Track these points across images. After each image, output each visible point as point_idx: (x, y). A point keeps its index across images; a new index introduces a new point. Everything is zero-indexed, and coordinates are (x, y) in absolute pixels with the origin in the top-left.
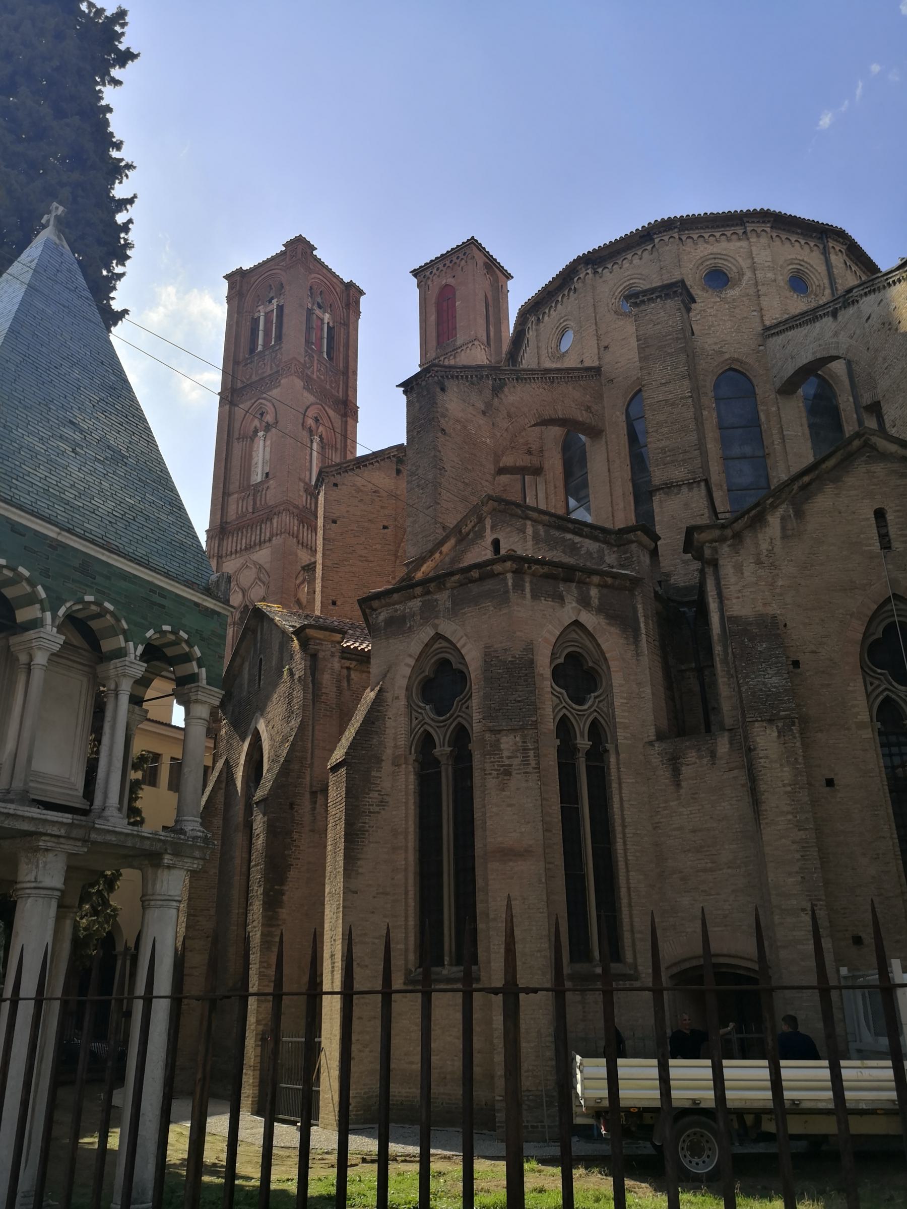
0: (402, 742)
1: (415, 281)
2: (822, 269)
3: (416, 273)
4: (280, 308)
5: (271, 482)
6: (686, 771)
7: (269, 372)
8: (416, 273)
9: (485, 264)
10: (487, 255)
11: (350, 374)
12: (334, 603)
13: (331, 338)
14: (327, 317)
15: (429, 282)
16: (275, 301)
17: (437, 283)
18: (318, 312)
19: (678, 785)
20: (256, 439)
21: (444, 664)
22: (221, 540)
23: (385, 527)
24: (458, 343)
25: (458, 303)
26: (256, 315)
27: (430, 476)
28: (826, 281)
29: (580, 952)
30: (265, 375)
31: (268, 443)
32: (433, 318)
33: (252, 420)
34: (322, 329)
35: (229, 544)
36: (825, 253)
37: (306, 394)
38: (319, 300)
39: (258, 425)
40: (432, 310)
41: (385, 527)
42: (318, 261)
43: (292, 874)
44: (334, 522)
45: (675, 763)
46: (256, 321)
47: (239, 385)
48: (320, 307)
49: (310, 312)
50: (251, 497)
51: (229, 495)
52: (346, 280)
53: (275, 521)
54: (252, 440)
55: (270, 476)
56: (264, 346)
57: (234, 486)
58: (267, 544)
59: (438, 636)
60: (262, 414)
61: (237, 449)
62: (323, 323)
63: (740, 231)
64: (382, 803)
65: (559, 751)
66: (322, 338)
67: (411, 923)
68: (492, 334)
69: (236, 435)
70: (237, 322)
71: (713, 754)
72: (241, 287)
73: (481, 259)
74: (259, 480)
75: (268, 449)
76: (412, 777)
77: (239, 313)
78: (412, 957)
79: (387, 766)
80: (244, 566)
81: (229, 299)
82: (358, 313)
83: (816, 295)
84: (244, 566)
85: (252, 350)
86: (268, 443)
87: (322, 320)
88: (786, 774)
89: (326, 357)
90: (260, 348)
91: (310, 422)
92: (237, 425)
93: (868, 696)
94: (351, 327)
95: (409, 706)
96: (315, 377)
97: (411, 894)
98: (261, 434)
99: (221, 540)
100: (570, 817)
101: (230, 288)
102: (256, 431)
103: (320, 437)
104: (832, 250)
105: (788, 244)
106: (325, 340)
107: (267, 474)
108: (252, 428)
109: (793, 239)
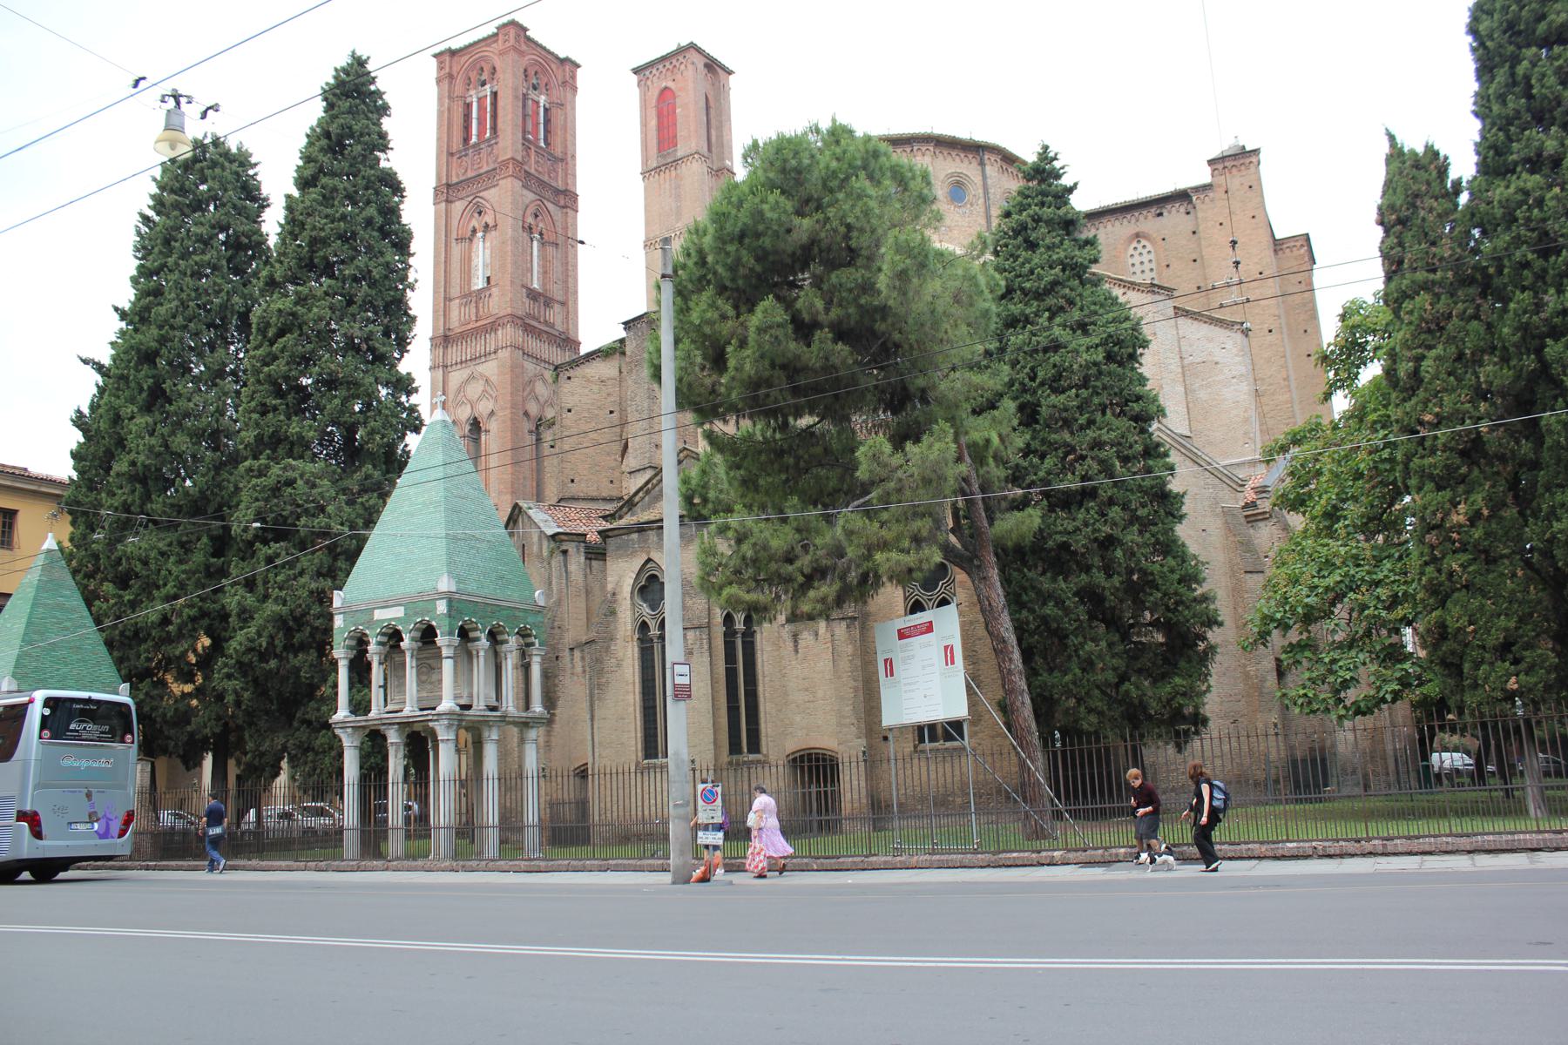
0: (629, 627)
1: (635, 78)
2: (978, 179)
3: (636, 71)
4: (495, 95)
5: (494, 289)
6: (802, 643)
7: (485, 169)
8: (636, 71)
9: (706, 66)
10: (707, 56)
11: (569, 159)
12: (572, 481)
13: (547, 121)
14: (542, 99)
15: (649, 83)
16: (487, 87)
17: (658, 83)
18: (532, 94)
19: (796, 651)
20: (475, 240)
21: (653, 578)
22: (445, 348)
23: (611, 412)
24: (679, 154)
25: (678, 111)
26: (468, 100)
27: (646, 405)
28: (981, 191)
29: (735, 747)
30: (482, 171)
31: (488, 244)
32: (653, 123)
33: (470, 220)
34: (538, 114)
35: (454, 354)
36: (982, 164)
37: (525, 192)
38: (535, 82)
39: (477, 226)
40: (653, 114)
41: (611, 412)
42: (529, 39)
43: (560, 703)
44: (569, 411)
45: (795, 637)
46: (468, 106)
47: (455, 180)
48: (535, 88)
49: (525, 96)
50: (473, 304)
51: (450, 300)
52: (562, 56)
53: (500, 332)
54: (471, 240)
55: (492, 283)
56: (478, 136)
57: (455, 291)
58: (493, 356)
59: (649, 560)
60: (480, 213)
61: (456, 250)
62: (538, 107)
63: (908, 150)
64: (619, 665)
65: (725, 634)
66: (539, 124)
67: (639, 735)
68: (714, 139)
69: (454, 236)
70: (449, 109)
71: (817, 635)
72: (451, 68)
73: (700, 62)
74: (480, 286)
75: (488, 252)
76: (636, 649)
77: (450, 97)
78: (640, 754)
79: (620, 642)
80: (471, 378)
81: (439, 81)
82: (575, 89)
83: (972, 205)
84: (471, 378)
85: (466, 139)
86: (488, 244)
87: (537, 103)
88: (850, 649)
89: (542, 144)
90: (474, 139)
91: (530, 220)
92: (455, 223)
93: (906, 599)
94: (569, 108)
95: (633, 604)
96: (533, 171)
97: (638, 718)
98: (480, 234)
99: (445, 348)
100: (731, 674)
101: (440, 68)
102: (474, 231)
103: (541, 234)
104: (987, 162)
105: (949, 159)
106: (542, 126)
107: (488, 278)
108: (470, 228)
109: (954, 154)
